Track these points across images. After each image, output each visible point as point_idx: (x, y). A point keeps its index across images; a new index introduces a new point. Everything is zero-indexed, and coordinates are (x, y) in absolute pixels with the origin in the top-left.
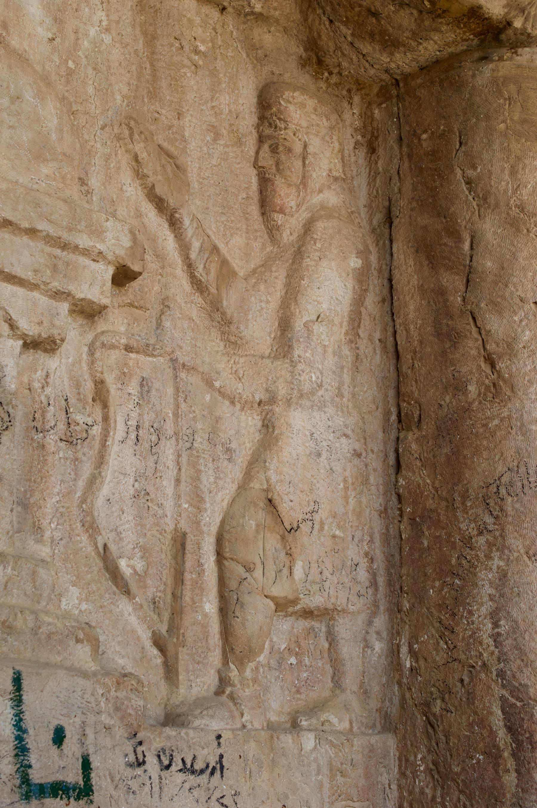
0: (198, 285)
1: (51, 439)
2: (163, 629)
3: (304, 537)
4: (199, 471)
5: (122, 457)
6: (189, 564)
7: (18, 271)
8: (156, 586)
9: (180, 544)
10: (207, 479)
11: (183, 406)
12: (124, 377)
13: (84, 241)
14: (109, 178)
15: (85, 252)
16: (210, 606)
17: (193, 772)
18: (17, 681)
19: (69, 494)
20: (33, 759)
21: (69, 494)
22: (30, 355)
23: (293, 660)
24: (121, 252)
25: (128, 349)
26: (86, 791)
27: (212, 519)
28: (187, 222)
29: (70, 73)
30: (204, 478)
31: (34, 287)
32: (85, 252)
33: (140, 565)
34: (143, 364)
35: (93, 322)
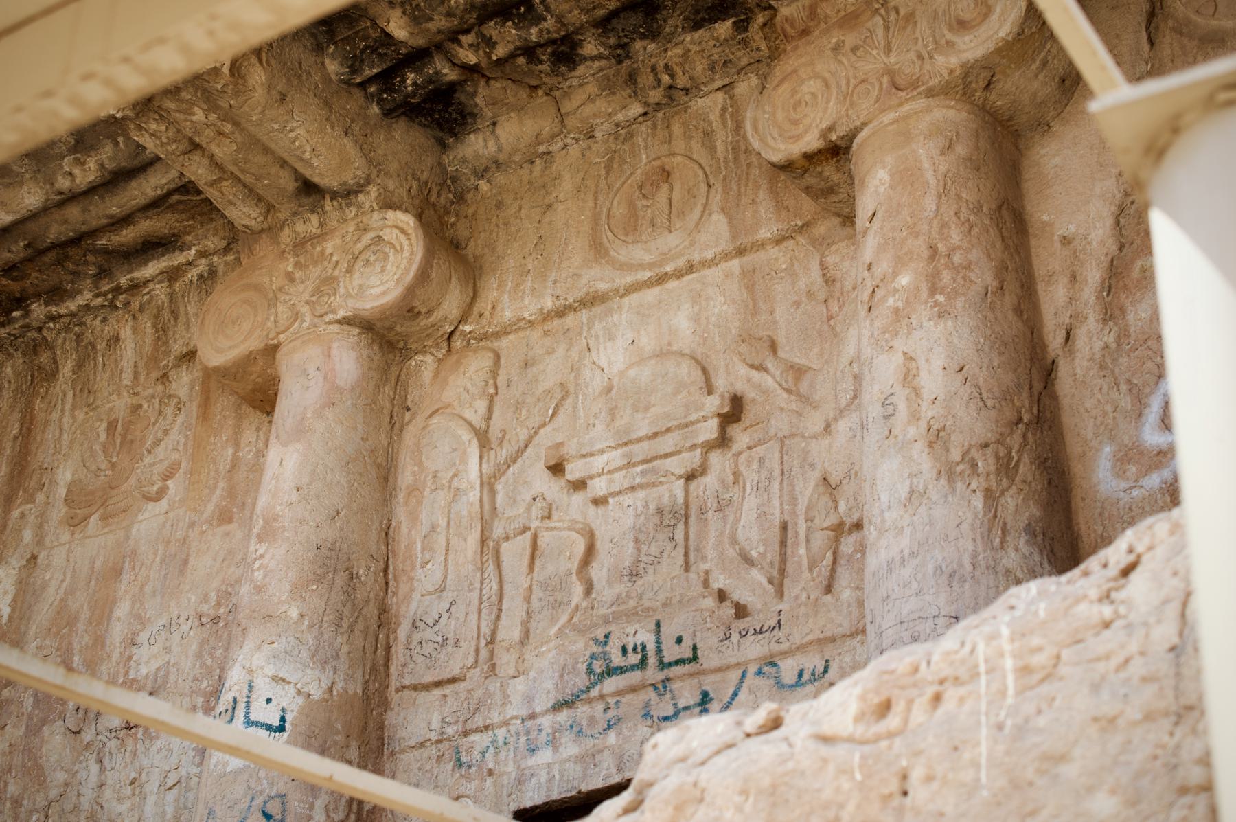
0: (788, 391)
1: (711, 513)
2: (775, 573)
3: (845, 487)
4: (794, 486)
5: (751, 503)
6: (789, 536)
7: (668, 451)
8: (773, 554)
9: (784, 527)
10: (799, 485)
11: (786, 458)
12: (749, 463)
13: (693, 417)
14: (728, 374)
15: (697, 421)
16: (802, 551)
17: (761, 632)
18: (658, 624)
19: (722, 534)
20: (665, 653)
21: (722, 534)
22: (693, 484)
23: (859, 555)
24: (714, 409)
25: (750, 448)
26: (694, 658)
27: (802, 507)
28: (770, 366)
29: (705, 339)
30: (797, 488)
31: (679, 452)
32: (697, 421)
33: (761, 549)
34: (761, 450)
35: (729, 447)
